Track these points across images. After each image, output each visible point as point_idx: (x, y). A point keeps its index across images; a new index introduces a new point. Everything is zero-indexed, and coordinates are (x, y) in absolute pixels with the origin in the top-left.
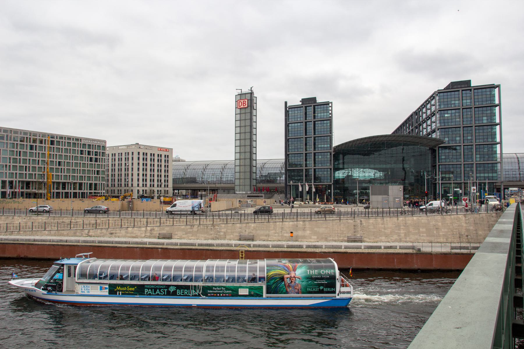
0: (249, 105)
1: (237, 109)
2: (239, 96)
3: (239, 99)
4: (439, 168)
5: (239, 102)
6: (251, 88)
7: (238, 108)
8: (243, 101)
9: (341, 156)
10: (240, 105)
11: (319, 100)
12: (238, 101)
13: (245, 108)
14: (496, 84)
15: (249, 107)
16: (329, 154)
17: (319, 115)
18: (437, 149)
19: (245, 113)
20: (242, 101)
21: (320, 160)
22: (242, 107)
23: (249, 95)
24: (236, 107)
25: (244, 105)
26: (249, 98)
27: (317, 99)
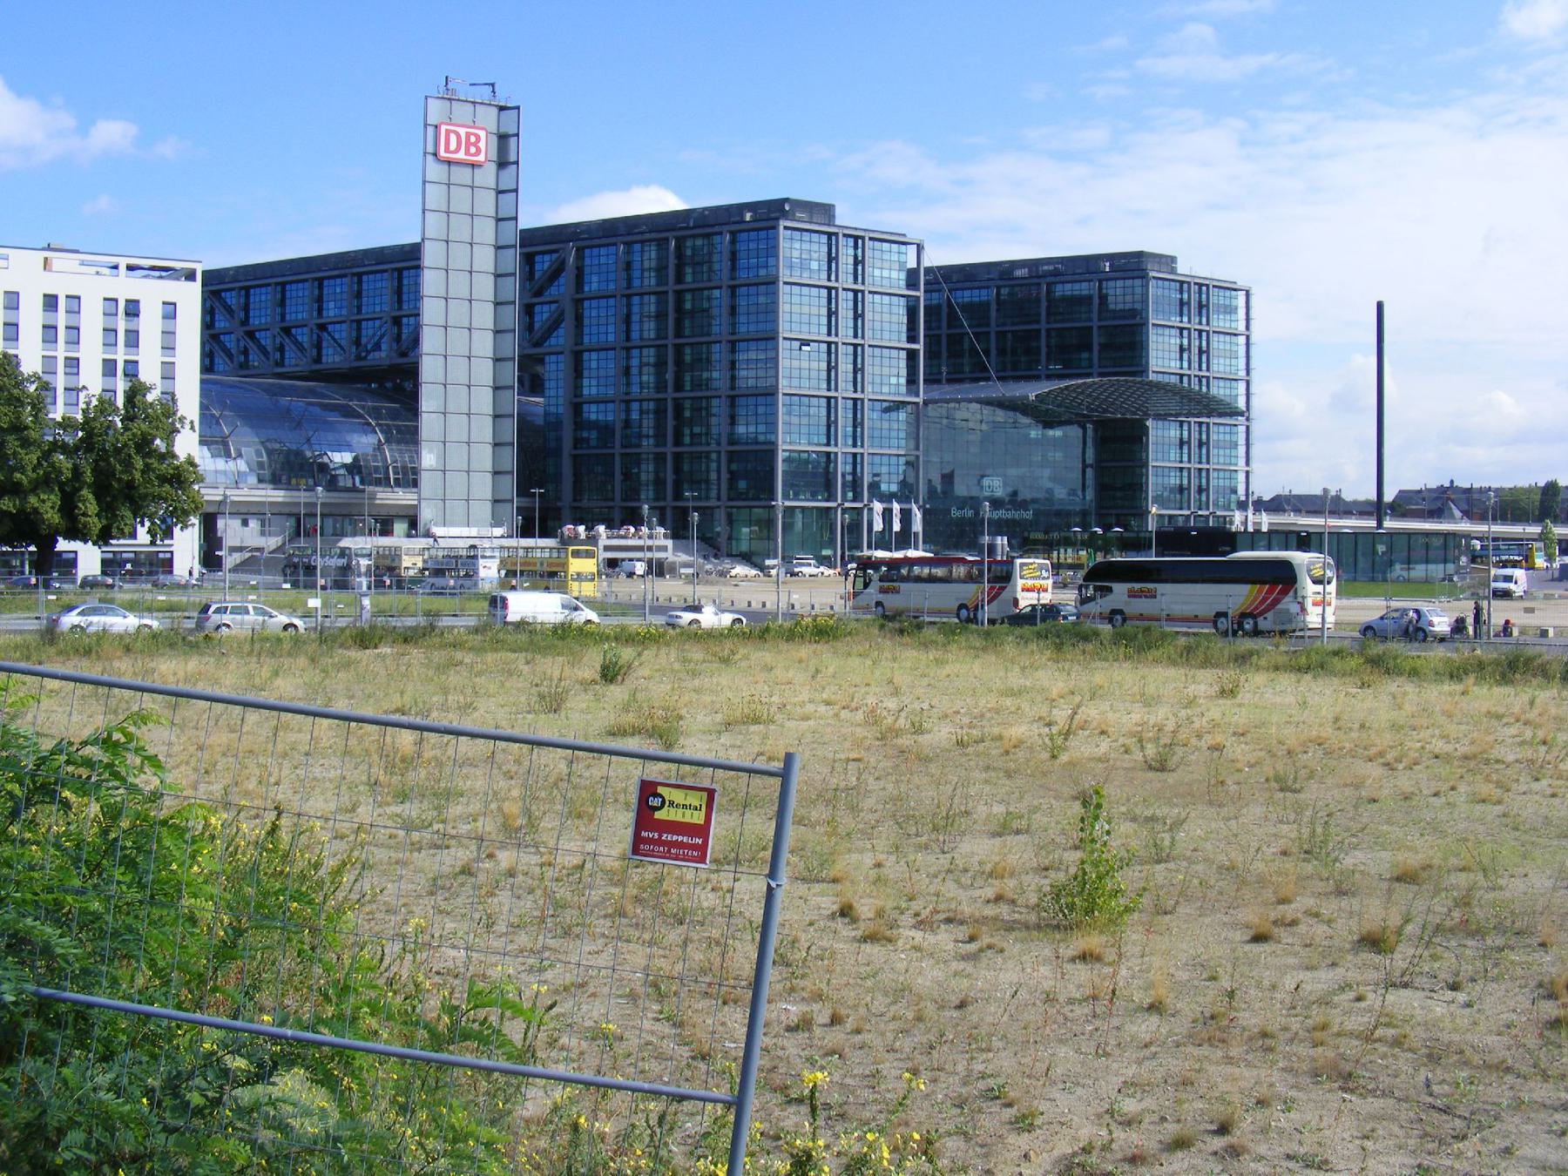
0: (493, 155)
8: (468, 135)
10: (453, 146)
13: (473, 165)
14: (1241, 284)
15: (492, 167)
17: (877, 272)
18: (1149, 423)
20: (462, 131)
22: (461, 155)
25: (473, 150)
27: (838, 212)
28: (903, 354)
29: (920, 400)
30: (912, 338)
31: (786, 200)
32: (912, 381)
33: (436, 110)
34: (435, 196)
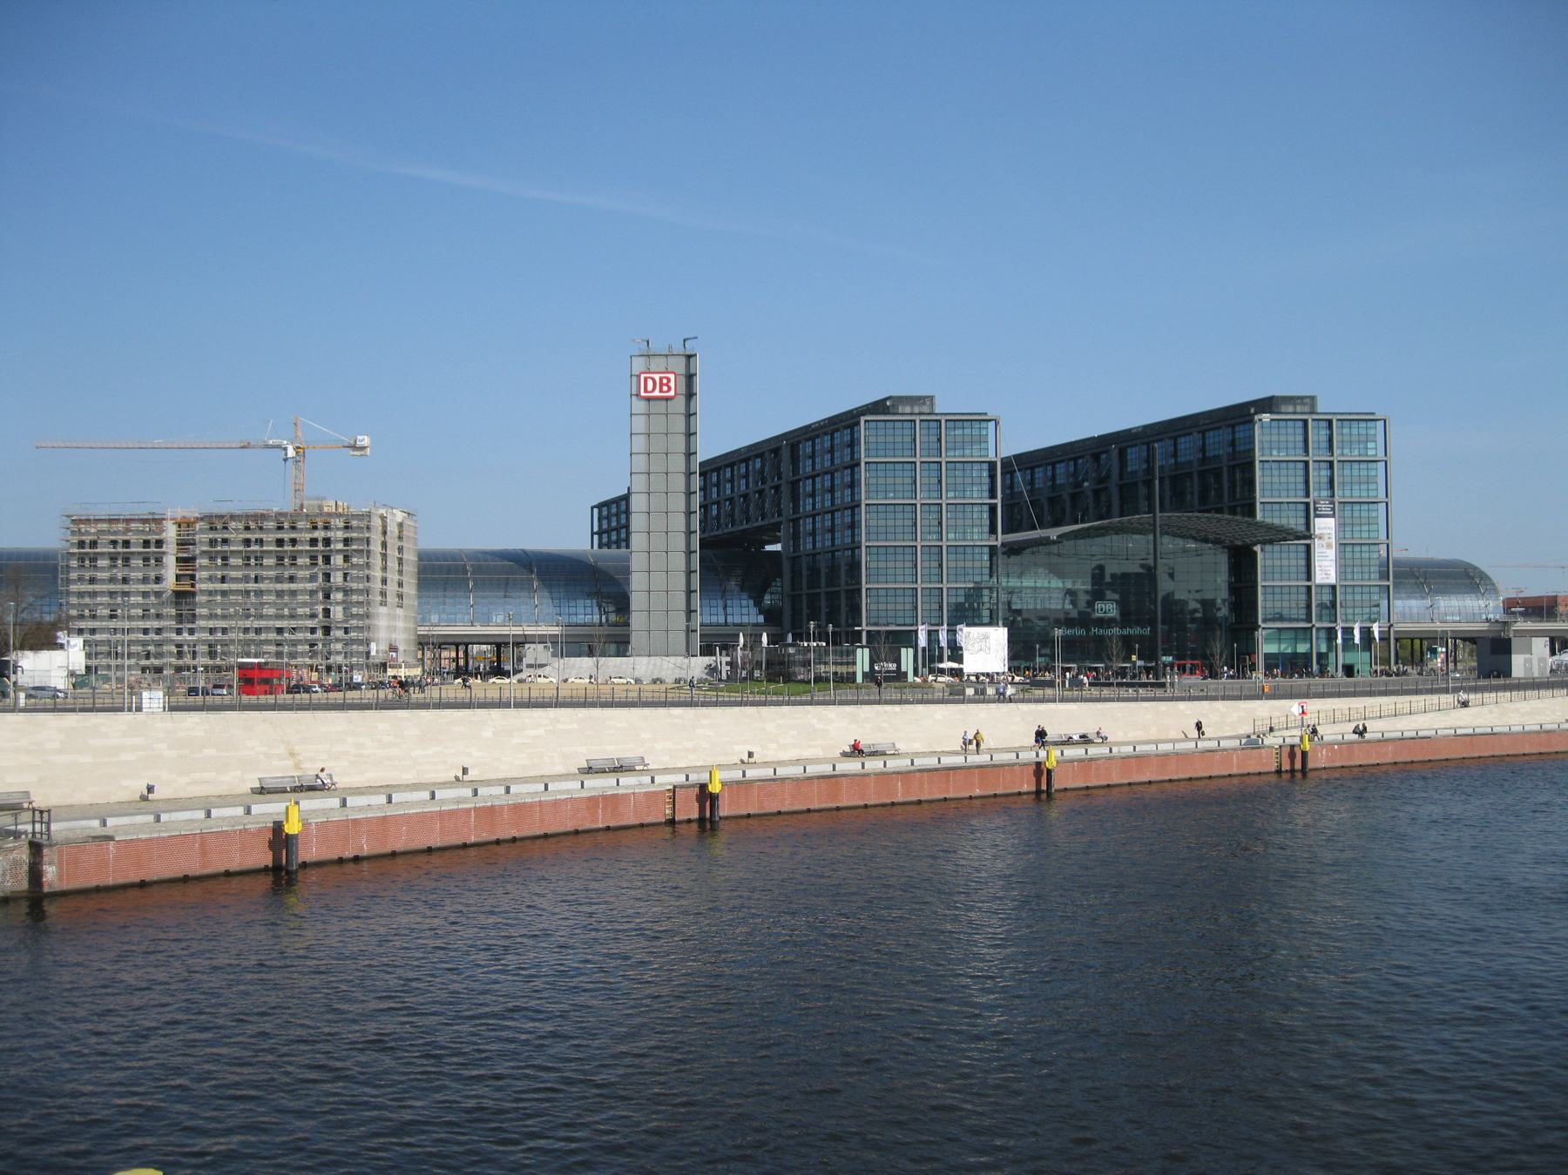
0: (682, 389)
3: (643, 370)
6: (685, 341)
8: (661, 379)
10: (650, 387)
11: (945, 405)
13: (667, 399)
15: (681, 400)
16: (986, 550)
18: (1257, 548)
20: (657, 377)
22: (657, 393)
23: (683, 360)
25: (665, 388)
26: (682, 370)
27: (937, 401)
28: (986, 508)
29: (999, 543)
30: (993, 495)
31: (889, 398)
32: (993, 530)
33: (639, 365)
34: (640, 424)
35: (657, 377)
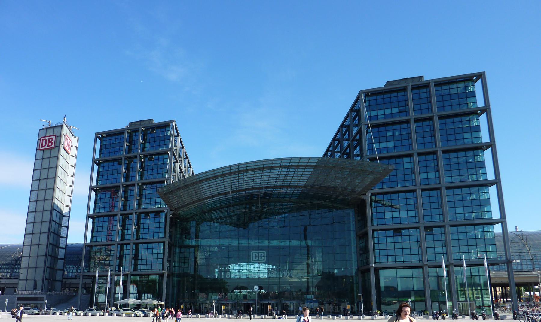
1: (38, 151)
2: (45, 130)
3: (45, 136)
4: (374, 238)
5: (43, 140)
7: (40, 150)
8: (49, 139)
9: (193, 223)
12: (42, 139)
13: (51, 149)
18: (367, 198)
19: (50, 158)
20: (47, 138)
21: (146, 226)
22: (46, 147)
24: (38, 148)
25: (50, 144)
35: (47, 138)
